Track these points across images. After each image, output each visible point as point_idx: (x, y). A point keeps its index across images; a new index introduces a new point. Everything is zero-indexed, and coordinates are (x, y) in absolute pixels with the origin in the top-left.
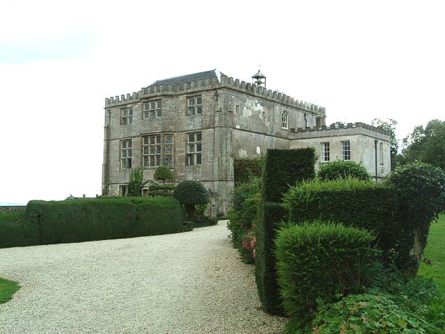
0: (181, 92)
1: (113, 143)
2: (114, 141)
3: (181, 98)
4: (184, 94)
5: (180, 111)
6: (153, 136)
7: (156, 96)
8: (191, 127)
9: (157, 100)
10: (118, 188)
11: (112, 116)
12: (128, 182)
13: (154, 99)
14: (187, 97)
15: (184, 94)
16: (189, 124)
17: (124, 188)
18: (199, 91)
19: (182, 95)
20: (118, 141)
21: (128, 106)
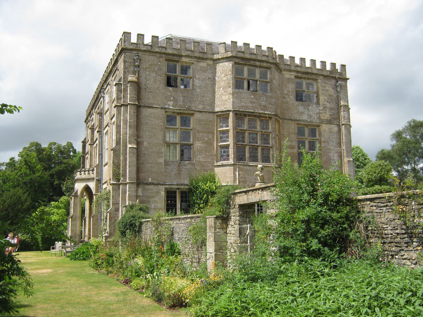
0: (287, 68)
1: (146, 112)
2: (149, 110)
3: (287, 75)
4: (294, 71)
5: (286, 92)
6: (253, 116)
7: (267, 62)
8: (305, 117)
9: (260, 67)
10: (163, 193)
11: (144, 66)
12: (186, 182)
13: (258, 63)
14: (296, 77)
15: (294, 71)
16: (302, 113)
17: (170, 196)
18: (316, 74)
19: (290, 71)
20: (163, 111)
21: (184, 59)
